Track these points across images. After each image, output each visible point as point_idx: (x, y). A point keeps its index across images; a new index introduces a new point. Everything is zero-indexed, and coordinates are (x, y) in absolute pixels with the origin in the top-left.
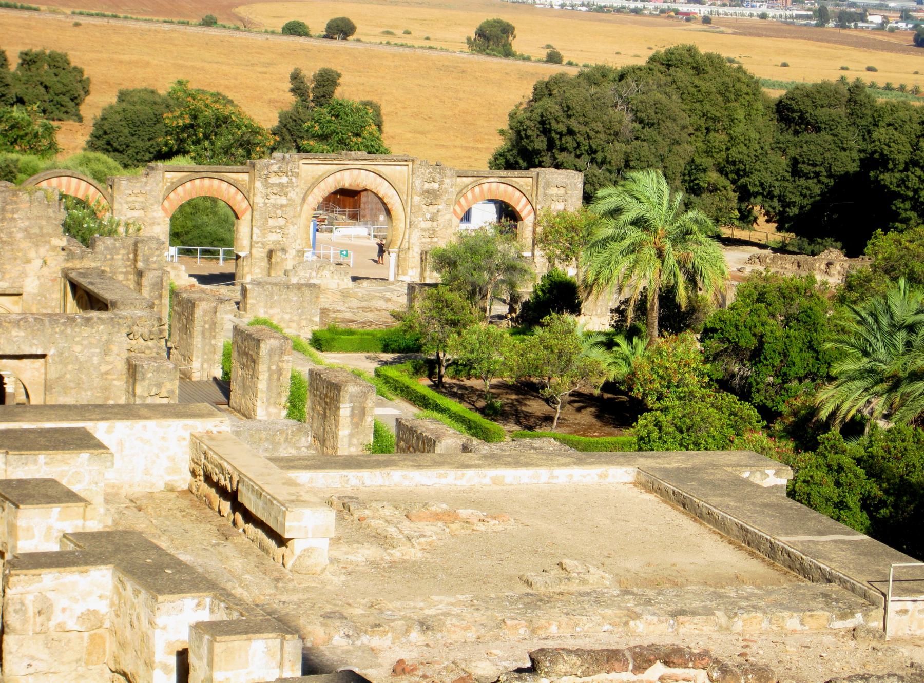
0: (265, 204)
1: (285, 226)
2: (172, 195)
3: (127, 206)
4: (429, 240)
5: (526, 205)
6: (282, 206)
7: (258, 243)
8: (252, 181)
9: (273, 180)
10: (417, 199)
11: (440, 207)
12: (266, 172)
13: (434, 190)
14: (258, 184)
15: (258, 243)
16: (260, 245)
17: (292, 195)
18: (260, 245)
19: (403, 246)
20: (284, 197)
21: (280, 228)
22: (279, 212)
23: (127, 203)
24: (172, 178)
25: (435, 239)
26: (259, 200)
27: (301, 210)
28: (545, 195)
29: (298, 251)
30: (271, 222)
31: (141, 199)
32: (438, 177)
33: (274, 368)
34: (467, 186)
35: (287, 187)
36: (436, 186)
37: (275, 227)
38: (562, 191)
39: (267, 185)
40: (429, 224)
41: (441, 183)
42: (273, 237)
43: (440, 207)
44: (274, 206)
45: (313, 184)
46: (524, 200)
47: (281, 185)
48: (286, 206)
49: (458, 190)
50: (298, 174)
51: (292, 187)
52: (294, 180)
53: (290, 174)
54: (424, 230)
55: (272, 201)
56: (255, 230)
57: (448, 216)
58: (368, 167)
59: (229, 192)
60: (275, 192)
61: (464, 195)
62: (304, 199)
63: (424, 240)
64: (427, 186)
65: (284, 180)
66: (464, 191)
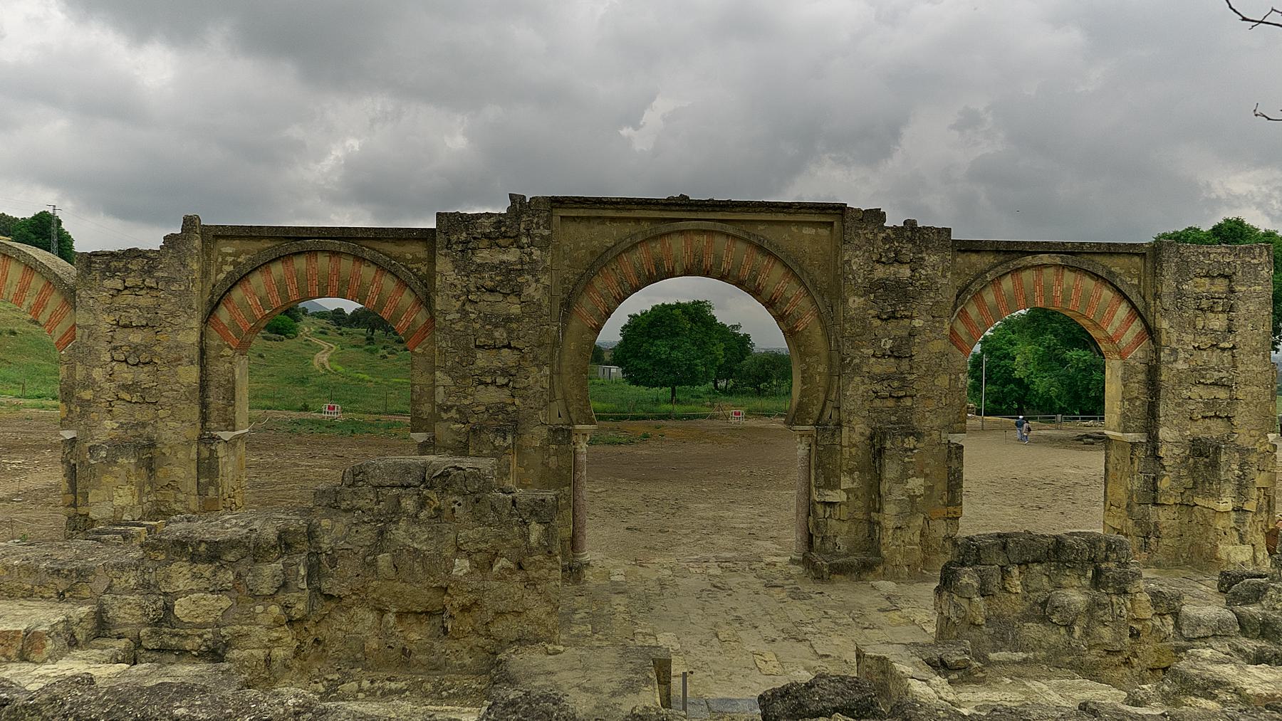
0: (464, 314)
1: (519, 367)
3: (110, 319)
4: (891, 403)
5: (1128, 322)
6: (508, 319)
7: (449, 409)
8: (432, 261)
9: (484, 255)
10: (855, 302)
11: (917, 323)
13: (898, 281)
14: (444, 265)
15: (449, 409)
16: (453, 413)
17: (533, 291)
18: (453, 413)
19: (826, 417)
20: (512, 298)
21: (505, 372)
22: (500, 334)
23: (109, 311)
24: (236, 254)
25: (908, 402)
28: (1180, 294)
29: (555, 431)
30: (482, 359)
31: (145, 300)
34: (982, 273)
35: (521, 272)
36: (905, 272)
38: (1220, 286)
39: (464, 267)
40: (888, 366)
41: (915, 264)
42: (490, 396)
43: (917, 323)
44: (486, 319)
45: (592, 267)
46: (1123, 311)
47: (507, 271)
48: (518, 319)
49: (959, 283)
50: (547, 240)
51: (533, 272)
52: (537, 253)
53: (524, 240)
54: (882, 379)
57: (939, 346)
59: (380, 289)
60: (489, 284)
61: (977, 296)
62: (568, 305)
63: (877, 403)
64: (880, 272)
65: (512, 256)
66: (975, 287)
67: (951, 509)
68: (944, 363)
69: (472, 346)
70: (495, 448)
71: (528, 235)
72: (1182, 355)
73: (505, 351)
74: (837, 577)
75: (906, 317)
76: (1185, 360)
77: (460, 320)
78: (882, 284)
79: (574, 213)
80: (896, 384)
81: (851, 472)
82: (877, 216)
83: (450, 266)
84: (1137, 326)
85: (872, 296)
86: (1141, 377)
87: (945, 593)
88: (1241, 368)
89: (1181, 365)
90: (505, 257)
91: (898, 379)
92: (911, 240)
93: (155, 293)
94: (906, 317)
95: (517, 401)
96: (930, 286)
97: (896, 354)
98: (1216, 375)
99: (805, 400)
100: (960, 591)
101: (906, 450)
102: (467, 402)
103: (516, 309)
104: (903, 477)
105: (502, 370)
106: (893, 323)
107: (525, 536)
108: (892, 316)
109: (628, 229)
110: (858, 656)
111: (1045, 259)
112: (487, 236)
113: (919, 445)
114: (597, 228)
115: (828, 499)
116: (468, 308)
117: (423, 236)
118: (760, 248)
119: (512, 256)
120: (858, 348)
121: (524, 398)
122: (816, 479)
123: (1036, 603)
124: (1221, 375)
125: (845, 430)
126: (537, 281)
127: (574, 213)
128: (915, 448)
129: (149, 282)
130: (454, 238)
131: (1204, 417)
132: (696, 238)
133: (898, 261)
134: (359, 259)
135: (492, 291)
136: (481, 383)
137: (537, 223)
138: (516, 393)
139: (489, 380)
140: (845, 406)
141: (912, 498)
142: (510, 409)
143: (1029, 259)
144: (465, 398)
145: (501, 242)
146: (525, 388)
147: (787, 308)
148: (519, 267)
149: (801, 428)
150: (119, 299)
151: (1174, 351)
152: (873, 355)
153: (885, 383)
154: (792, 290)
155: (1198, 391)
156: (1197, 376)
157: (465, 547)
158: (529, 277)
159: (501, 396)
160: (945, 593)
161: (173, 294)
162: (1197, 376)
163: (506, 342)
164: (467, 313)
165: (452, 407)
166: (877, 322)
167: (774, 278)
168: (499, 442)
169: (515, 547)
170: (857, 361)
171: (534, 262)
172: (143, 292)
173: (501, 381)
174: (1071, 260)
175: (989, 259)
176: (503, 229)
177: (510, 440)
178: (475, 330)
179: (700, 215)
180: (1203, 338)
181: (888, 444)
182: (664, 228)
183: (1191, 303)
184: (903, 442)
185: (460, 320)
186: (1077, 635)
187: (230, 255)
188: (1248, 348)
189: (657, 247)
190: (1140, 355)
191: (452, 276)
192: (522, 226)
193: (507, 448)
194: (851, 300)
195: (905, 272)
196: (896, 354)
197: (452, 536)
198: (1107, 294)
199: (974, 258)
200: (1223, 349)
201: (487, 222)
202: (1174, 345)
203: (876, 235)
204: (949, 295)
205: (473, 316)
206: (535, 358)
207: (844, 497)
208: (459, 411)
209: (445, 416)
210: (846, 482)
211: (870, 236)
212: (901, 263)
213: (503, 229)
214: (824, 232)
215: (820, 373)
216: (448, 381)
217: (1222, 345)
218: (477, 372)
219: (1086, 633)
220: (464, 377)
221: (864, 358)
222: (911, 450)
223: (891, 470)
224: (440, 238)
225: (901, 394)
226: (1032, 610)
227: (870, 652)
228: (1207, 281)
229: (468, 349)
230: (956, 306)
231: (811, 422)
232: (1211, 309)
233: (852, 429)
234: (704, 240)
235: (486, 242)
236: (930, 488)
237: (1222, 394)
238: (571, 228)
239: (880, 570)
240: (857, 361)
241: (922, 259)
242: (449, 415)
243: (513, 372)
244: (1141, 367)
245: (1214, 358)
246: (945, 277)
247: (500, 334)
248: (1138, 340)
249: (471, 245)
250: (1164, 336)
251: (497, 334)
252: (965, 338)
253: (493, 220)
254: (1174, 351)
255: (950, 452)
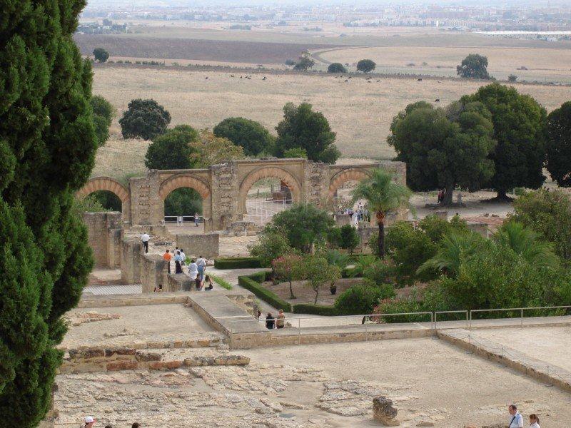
2: (164, 187)
6: (229, 190)
8: (210, 177)
9: (223, 176)
14: (214, 178)
21: (228, 203)
26: (214, 188)
30: (223, 200)
32: (319, 170)
33: (159, 275)
41: (321, 173)
47: (227, 178)
56: (213, 204)
64: (313, 175)
65: (229, 175)
78: (313, 178)
97: (317, 194)
103: (230, 188)
109: (254, 167)
119: (229, 175)
189: (261, 172)
204: (329, 180)
214: (299, 166)
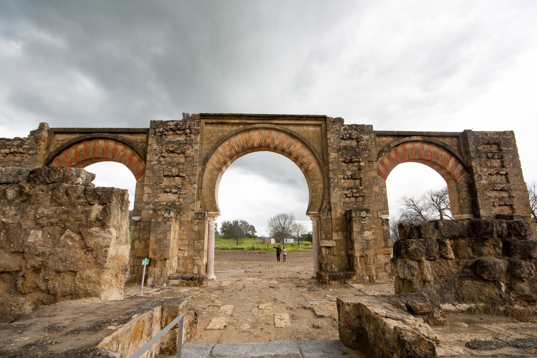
0: (159, 162)
4: (353, 199)
6: (179, 164)
9: (171, 137)
12: (161, 129)
14: (152, 141)
15: (149, 203)
16: (151, 206)
20: (181, 155)
21: (176, 187)
27: (203, 170)
28: (478, 151)
30: (166, 182)
37: (170, 187)
38: (494, 148)
41: (358, 140)
43: (362, 164)
44: (170, 164)
46: (452, 161)
47: (179, 143)
48: (183, 164)
49: (378, 149)
53: (188, 131)
55: (169, 159)
58: (278, 127)
60: (171, 149)
64: (343, 143)
65: (182, 138)
67: (386, 249)
68: (376, 182)
69: (162, 175)
70: (165, 218)
71: (190, 129)
72: (484, 177)
73: (177, 178)
74: (334, 283)
75: (357, 162)
76: (486, 179)
77: (157, 164)
78: (345, 148)
79: (210, 121)
80: (354, 191)
81: (337, 231)
82: (340, 121)
83: (155, 142)
84: (460, 167)
85: (341, 153)
86: (466, 189)
87: (399, 262)
88: (512, 183)
89: (484, 182)
90: (179, 139)
91: (355, 188)
92: (355, 130)
93: (22, 155)
94: (357, 162)
95: (181, 200)
96: (366, 148)
97: (353, 178)
98: (501, 186)
99: (314, 200)
100: (410, 255)
101: (362, 218)
102: (157, 200)
103: (182, 160)
104: (362, 230)
105: (175, 186)
106: (350, 165)
107: (87, 213)
108: (351, 162)
110: (338, 306)
111: (415, 138)
112: (172, 130)
113: (368, 215)
114: (220, 128)
115: (327, 245)
116: (162, 159)
117: (145, 132)
118: (291, 135)
119: (182, 138)
120: (336, 175)
121: (184, 198)
122: (321, 236)
123: (466, 267)
124: (503, 186)
125: (333, 212)
126: (193, 147)
127: (210, 121)
128: (366, 217)
129: (21, 150)
130: (157, 130)
131: (500, 205)
132: (263, 132)
133: (350, 138)
134: (116, 140)
135: (172, 152)
136: (165, 192)
137: (194, 124)
138: (180, 196)
139: (168, 191)
140: (333, 200)
141: (367, 241)
142: (177, 204)
143: (407, 139)
144: (157, 198)
145: (178, 132)
146: (185, 194)
147: (305, 160)
148: (185, 142)
149: (313, 212)
150: (7, 158)
151: (480, 176)
152: (344, 178)
153: (350, 191)
154: (305, 152)
155: (493, 194)
156: (492, 187)
157: (40, 221)
158: (189, 146)
159: (172, 197)
160: (399, 262)
161: (30, 155)
162: (492, 187)
163: (177, 173)
164: (161, 161)
165: (150, 203)
166: (343, 164)
167: (298, 147)
168: (166, 215)
169: (77, 219)
170: (336, 181)
171: (192, 140)
172: (18, 155)
173: (174, 190)
174: (427, 139)
175: (390, 139)
176: (179, 126)
177: (172, 214)
178: (163, 168)
179: (265, 121)
180: (492, 170)
181: (353, 215)
182: (249, 127)
183: (484, 155)
184: (360, 213)
185: (157, 164)
186: (503, 289)
187: (61, 141)
188: (513, 174)
190: (464, 179)
191: (155, 146)
192: (187, 125)
193: (171, 218)
194: (331, 154)
195: (354, 143)
196: (353, 178)
197: (33, 212)
198: (444, 154)
199: (384, 139)
200: (502, 175)
201: (171, 124)
202: (479, 173)
203: (340, 128)
205: (163, 163)
206: (190, 180)
207: (335, 244)
208: (153, 205)
209: (147, 207)
210: (335, 236)
211: (338, 128)
212: (353, 139)
213: (179, 126)
214: (318, 129)
215: (320, 188)
216: (150, 191)
217: (501, 173)
218: (163, 187)
219: (510, 288)
220: (157, 189)
221: (339, 179)
222: (364, 218)
223: (356, 228)
224: (151, 132)
225: (358, 195)
226: (464, 272)
227: (346, 301)
228: (488, 146)
229: (160, 177)
230: (378, 158)
231: (317, 210)
232: (493, 158)
233: (336, 212)
234: (266, 132)
235: (171, 132)
236: (376, 239)
237: (505, 194)
238: (209, 127)
239: (355, 278)
240: (336, 181)
241: (362, 137)
242: (149, 206)
243: (180, 186)
244: (465, 185)
245: (498, 179)
246: (372, 144)
247: (175, 171)
248: (461, 173)
249: (164, 133)
250: (474, 169)
251: (173, 170)
252: (384, 172)
253: (175, 123)
254: (480, 176)
255: (383, 222)
